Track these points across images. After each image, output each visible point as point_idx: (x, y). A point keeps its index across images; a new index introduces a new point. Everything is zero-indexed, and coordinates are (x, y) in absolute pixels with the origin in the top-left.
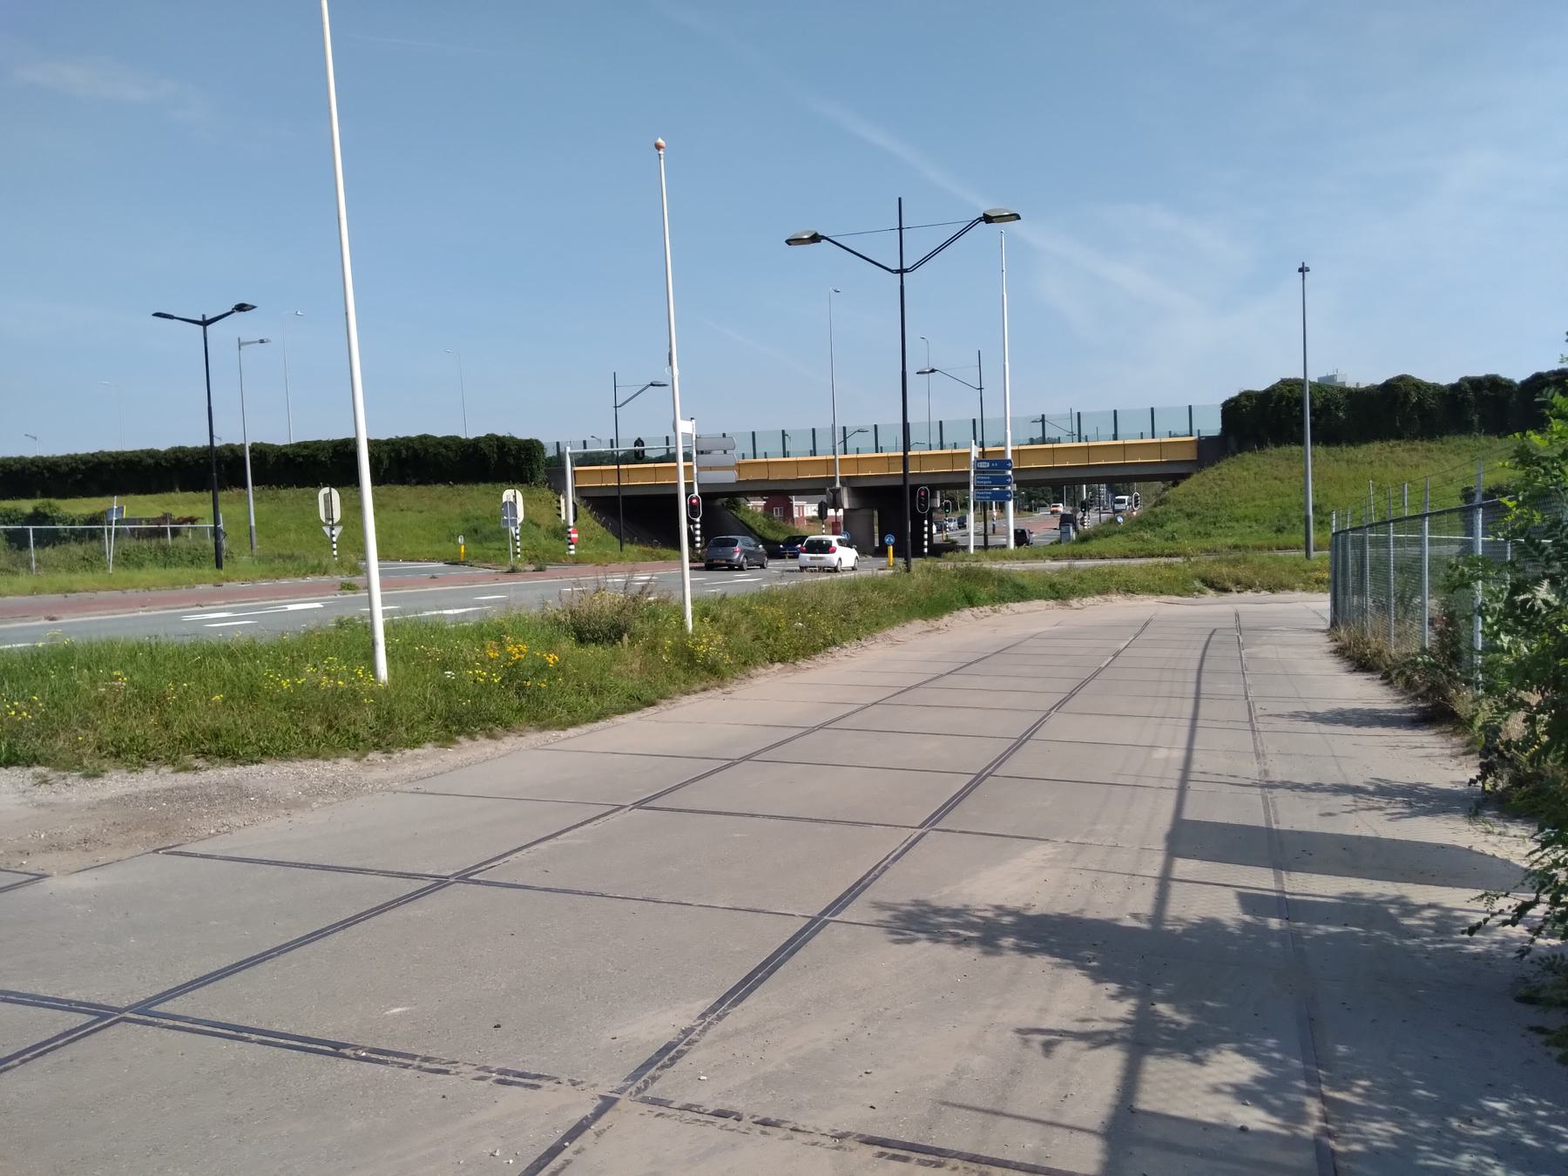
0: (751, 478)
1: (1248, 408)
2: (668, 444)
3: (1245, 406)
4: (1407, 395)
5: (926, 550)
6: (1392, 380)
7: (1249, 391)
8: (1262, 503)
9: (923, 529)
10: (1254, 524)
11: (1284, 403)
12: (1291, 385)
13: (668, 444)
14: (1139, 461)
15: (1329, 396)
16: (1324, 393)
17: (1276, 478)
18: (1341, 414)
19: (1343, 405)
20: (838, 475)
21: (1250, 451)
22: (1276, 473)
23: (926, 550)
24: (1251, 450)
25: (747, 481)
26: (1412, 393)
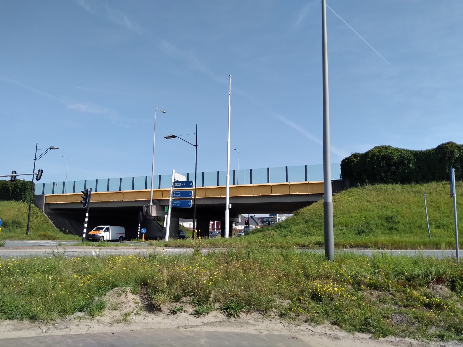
0: (115, 200)
1: (355, 162)
2: (34, 172)
3: (353, 161)
4: (452, 152)
5: (139, 236)
6: (440, 145)
7: (357, 153)
8: (353, 215)
9: (85, 220)
10: (344, 228)
11: (375, 158)
12: (380, 148)
13: (34, 172)
14: (297, 193)
15: (403, 155)
16: (400, 153)
17: (367, 201)
18: (411, 165)
19: (412, 160)
20: (152, 199)
21: (356, 187)
22: (368, 198)
23: (139, 236)
24: (356, 186)
25: (113, 202)
26: (456, 151)
